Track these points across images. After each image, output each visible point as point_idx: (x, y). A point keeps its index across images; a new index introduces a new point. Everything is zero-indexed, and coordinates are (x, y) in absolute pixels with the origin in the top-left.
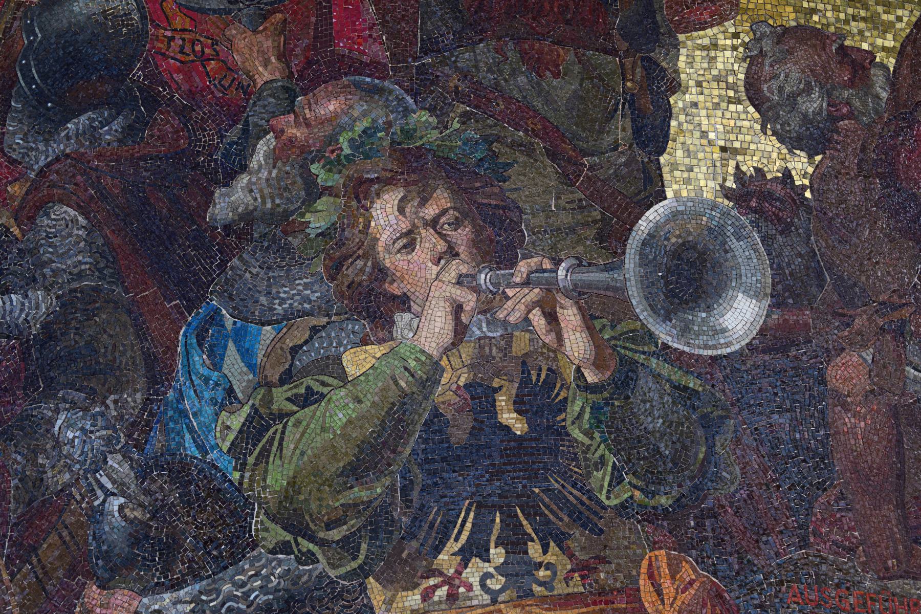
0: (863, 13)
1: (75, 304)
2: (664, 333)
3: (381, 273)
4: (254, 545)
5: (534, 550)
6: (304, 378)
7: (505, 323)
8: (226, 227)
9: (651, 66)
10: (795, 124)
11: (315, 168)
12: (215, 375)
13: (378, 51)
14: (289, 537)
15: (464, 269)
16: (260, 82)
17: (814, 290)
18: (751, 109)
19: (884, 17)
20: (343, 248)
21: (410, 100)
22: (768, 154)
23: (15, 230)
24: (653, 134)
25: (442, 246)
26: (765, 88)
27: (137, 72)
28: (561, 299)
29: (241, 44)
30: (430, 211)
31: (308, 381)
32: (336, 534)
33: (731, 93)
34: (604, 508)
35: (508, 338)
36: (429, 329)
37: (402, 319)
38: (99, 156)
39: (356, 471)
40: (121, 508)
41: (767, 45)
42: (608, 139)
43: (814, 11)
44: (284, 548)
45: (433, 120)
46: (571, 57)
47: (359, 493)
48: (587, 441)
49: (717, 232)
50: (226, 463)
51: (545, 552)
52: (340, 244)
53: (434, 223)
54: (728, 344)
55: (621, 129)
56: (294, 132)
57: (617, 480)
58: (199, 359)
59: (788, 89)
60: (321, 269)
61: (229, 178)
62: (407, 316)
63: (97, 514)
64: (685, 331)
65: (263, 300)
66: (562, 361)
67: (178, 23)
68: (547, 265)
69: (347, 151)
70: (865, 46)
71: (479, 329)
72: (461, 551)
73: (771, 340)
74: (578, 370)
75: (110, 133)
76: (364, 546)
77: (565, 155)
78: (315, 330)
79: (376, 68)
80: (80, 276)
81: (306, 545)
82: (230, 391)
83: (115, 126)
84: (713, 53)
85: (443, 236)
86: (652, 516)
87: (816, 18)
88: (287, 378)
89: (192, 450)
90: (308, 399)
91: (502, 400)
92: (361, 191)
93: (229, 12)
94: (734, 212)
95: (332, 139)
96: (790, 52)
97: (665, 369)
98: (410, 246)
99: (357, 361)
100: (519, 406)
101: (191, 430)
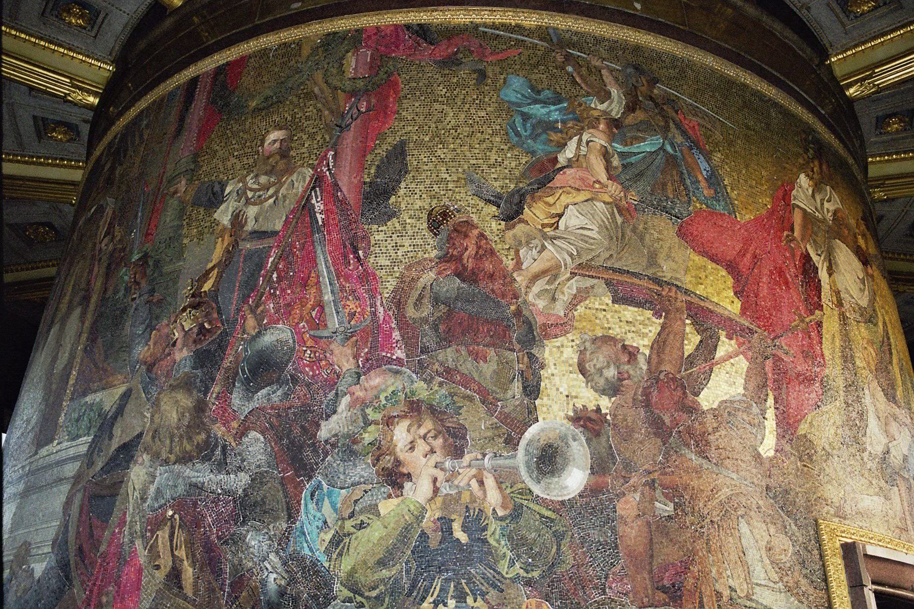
0: (633, 329)
1: (258, 479)
2: (537, 490)
3: (398, 463)
4: (335, 598)
5: (470, 600)
6: (359, 515)
7: (457, 487)
8: (326, 441)
9: (531, 356)
10: (601, 382)
11: (369, 411)
12: (318, 515)
13: (399, 354)
14: (352, 595)
15: (439, 460)
16: (344, 370)
17: (611, 465)
18: (581, 376)
19: (643, 330)
20: (379, 450)
21: (414, 376)
22: (588, 398)
23: (233, 444)
24: (532, 390)
25: (428, 448)
26: (587, 366)
27: (290, 367)
28: (485, 473)
29: (336, 352)
30: (422, 431)
31: (361, 518)
32: (374, 594)
33: (571, 369)
34: (506, 579)
35: (460, 493)
36: (418, 491)
37: (408, 485)
38: (272, 408)
39: (382, 563)
40: (275, 579)
41: (588, 344)
42: (510, 393)
43: (610, 328)
44: (350, 600)
45: (425, 386)
46: (493, 353)
47: (385, 573)
48: (497, 545)
49: (563, 438)
50: (323, 559)
51: (475, 601)
52: (379, 448)
53: (424, 437)
54: (569, 494)
55: (516, 388)
56: (360, 394)
57: (512, 564)
58: (312, 506)
59: (598, 367)
60: (369, 461)
61: (328, 417)
62: (410, 484)
63: (264, 583)
64: (547, 488)
65: (342, 477)
66: (486, 505)
67: (308, 344)
68: (480, 457)
69: (384, 402)
70: (635, 345)
71: (445, 490)
72: (434, 602)
73: (592, 491)
74: (494, 510)
75: (275, 398)
76: (387, 599)
77: (488, 399)
78: (366, 492)
79: (399, 361)
80: (259, 466)
81: (359, 599)
82: (325, 522)
83: (279, 393)
84: (562, 349)
85: (428, 444)
86: (529, 583)
87: (611, 331)
88: (352, 515)
89: (307, 551)
90: (361, 526)
91: (456, 526)
92: (389, 422)
93: (332, 337)
94: (572, 427)
95: (377, 397)
96: (599, 348)
97: (537, 508)
98: (412, 449)
99: (387, 507)
100: (465, 528)
101: (307, 542)
